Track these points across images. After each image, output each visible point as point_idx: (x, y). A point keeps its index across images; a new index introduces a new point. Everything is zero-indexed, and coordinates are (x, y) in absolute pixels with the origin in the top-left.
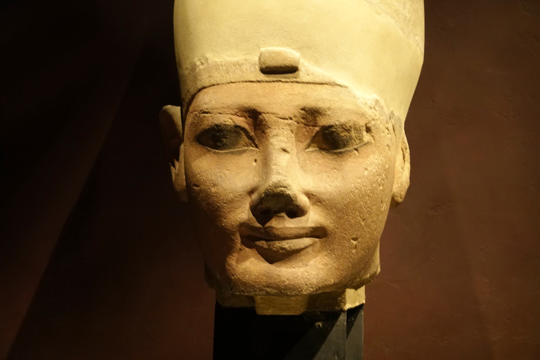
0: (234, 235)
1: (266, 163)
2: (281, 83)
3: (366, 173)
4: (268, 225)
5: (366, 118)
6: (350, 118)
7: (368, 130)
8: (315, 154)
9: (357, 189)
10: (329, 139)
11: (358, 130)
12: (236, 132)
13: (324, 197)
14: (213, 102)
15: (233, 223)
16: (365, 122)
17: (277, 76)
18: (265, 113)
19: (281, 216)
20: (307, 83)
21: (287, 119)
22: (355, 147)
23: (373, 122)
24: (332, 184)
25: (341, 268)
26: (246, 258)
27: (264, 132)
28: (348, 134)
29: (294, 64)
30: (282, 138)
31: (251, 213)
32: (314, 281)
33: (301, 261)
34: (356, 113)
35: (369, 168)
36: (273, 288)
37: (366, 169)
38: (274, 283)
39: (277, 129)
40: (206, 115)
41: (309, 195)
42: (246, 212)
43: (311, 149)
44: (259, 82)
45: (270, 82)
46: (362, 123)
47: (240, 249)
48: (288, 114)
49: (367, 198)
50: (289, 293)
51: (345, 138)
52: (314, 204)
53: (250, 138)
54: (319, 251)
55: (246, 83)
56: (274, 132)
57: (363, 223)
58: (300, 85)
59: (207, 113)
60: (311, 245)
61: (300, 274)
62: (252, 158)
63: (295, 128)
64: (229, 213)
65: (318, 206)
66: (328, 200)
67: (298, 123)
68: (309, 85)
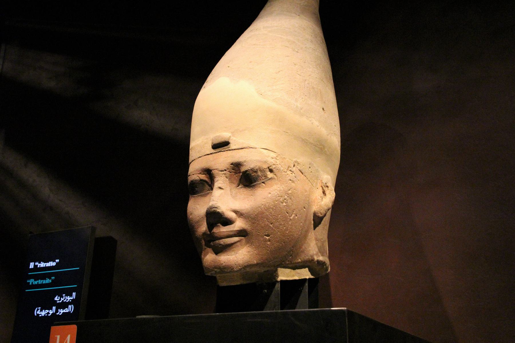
3: (270, 195)
7: (271, 171)
11: (263, 171)
13: (244, 212)
23: (274, 166)
29: (227, 140)
32: (241, 262)
33: (234, 251)
37: (270, 193)
41: (236, 212)
43: (240, 186)
44: (211, 154)
46: (265, 166)
52: (239, 217)
58: (231, 151)
60: (238, 241)
63: (228, 175)
68: (235, 151)
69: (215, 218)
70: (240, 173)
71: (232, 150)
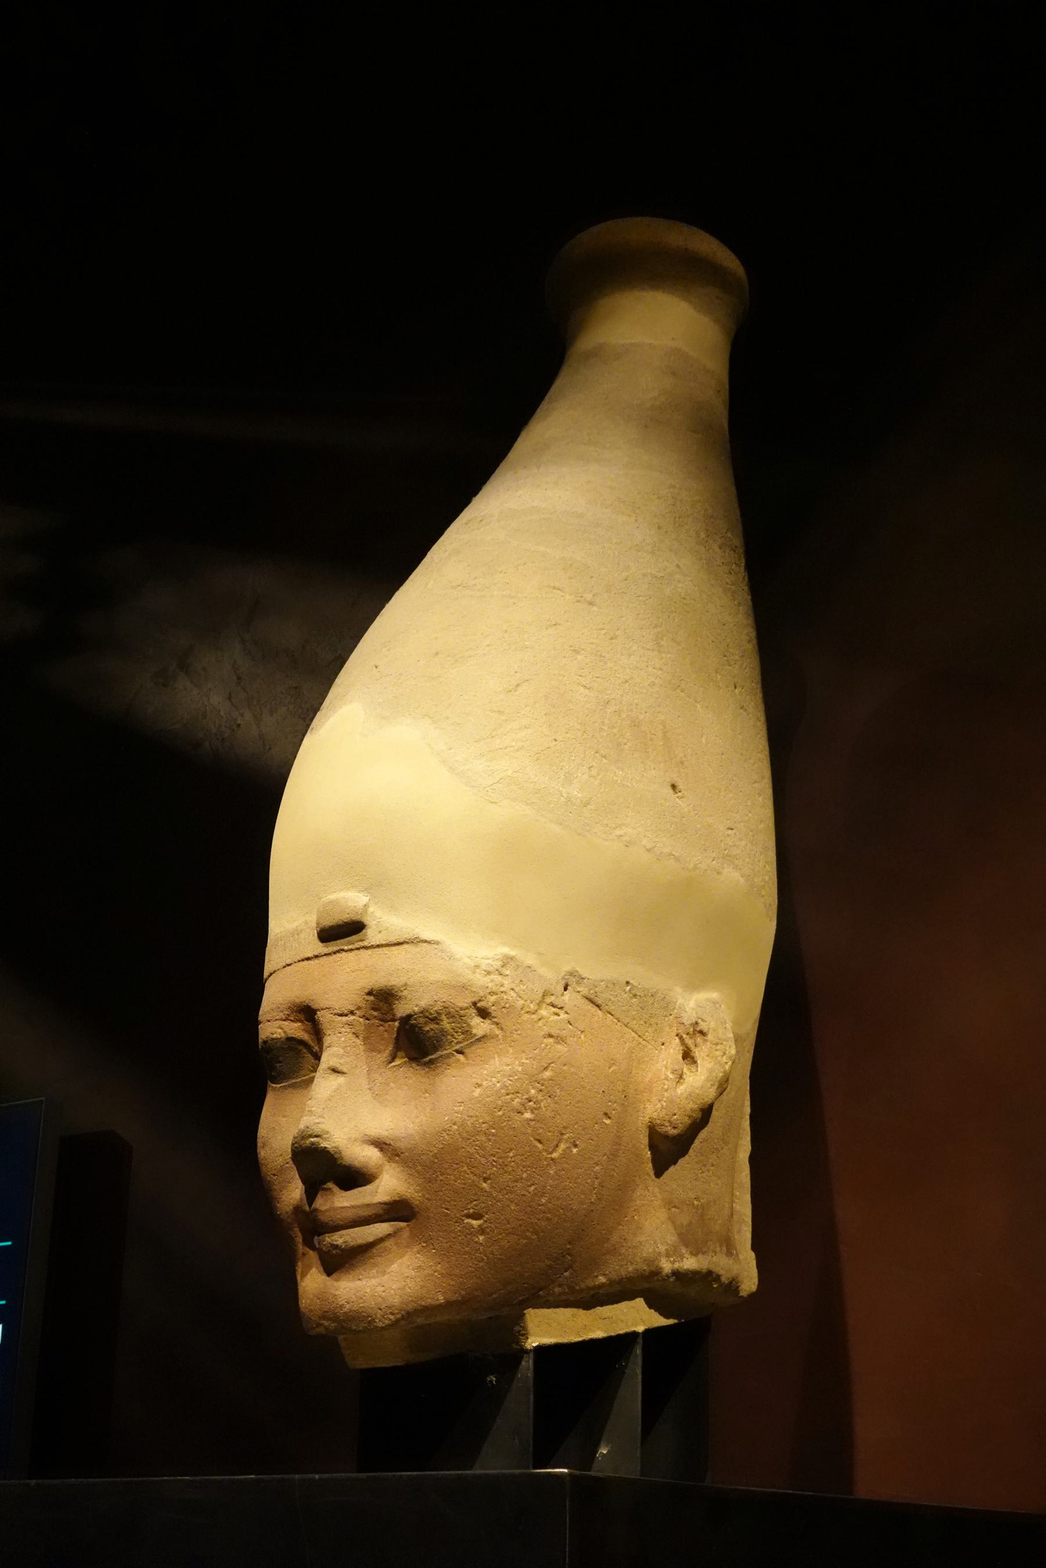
3: (478, 1091)
7: (484, 1013)
11: (456, 1015)
13: (402, 1145)
15: (288, 1210)
20: (378, 946)
21: (346, 1015)
22: (457, 1047)
23: (493, 999)
29: (355, 918)
32: (396, 1301)
33: (375, 1265)
35: (484, 1083)
37: (479, 1086)
41: (379, 1144)
43: (397, 1062)
44: (316, 957)
46: (463, 1001)
51: (431, 1033)
52: (390, 1160)
58: (369, 952)
60: (389, 1236)
61: (368, 1290)
63: (360, 1028)
65: (396, 1162)
68: (380, 949)
70: (394, 1020)
71: (372, 947)
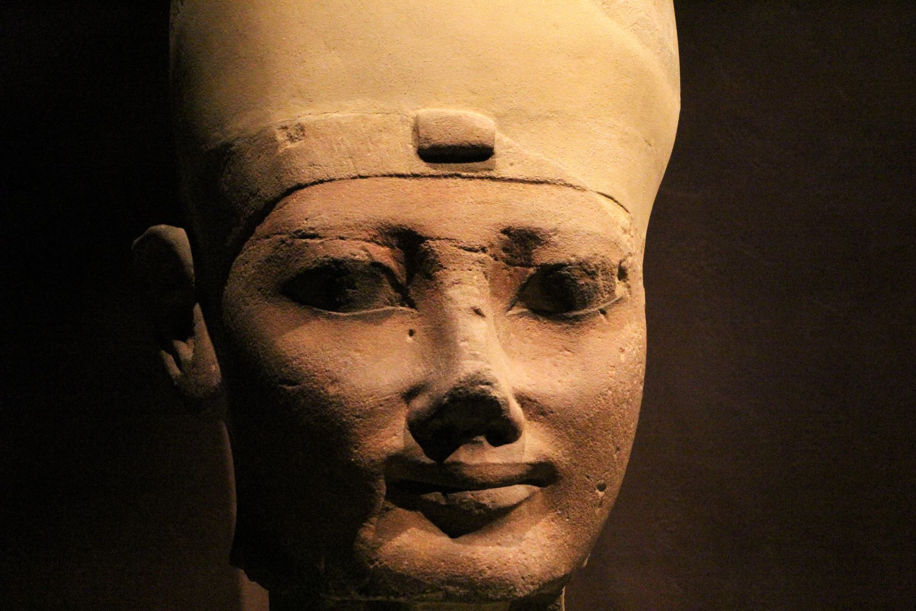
0: (374, 480)
1: (441, 337)
2: (459, 180)
3: (623, 357)
4: (451, 458)
5: (621, 250)
6: (595, 251)
8: (525, 319)
9: (610, 389)
10: (552, 291)
12: (373, 275)
14: (325, 216)
15: (373, 456)
16: (619, 259)
17: (453, 165)
18: (432, 239)
19: (477, 442)
20: (511, 180)
21: (476, 251)
22: (602, 307)
24: (565, 380)
25: (576, 544)
26: (400, 528)
27: (430, 277)
28: (592, 281)
30: (470, 287)
31: (410, 436)
32: (536, 570)
33: (511, 530)
34: (603, 240)
35: (626, 348)
36: (462, 585)
37: (623, 351)
38: (463, 575)
39: (459, 271)
40: (308, 240)
41: (524, 400)
42: (400, 434)
43: (516, 311)
44: (416, 176)
45: (438, 177)
47: (388, 509)
48: (477, 242)
49: (625, 406)
50: (490, 595)
51: (585, 288)
52: (530, 418)
53: (397, 287)
54: (544, 513)
55: (390, 179)
56: (454, 276)
57: (615, 456)
58: (498, 184)
59: (313, 237)
61: (511, 556)
62: (403, 329)
64: (365, 436)
65: (540, 421)
66: (561, 410)
67: (496, 259)
68: (513, 185)
69: (476, 415)
70: (530, 266)
71: (503, 180)
